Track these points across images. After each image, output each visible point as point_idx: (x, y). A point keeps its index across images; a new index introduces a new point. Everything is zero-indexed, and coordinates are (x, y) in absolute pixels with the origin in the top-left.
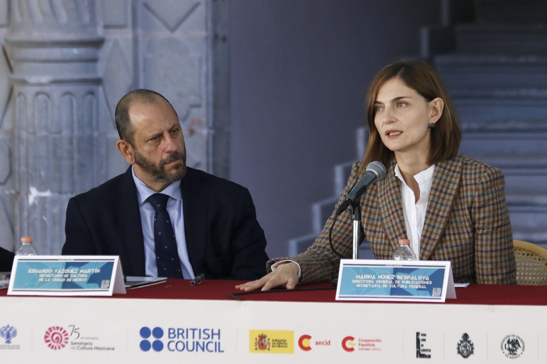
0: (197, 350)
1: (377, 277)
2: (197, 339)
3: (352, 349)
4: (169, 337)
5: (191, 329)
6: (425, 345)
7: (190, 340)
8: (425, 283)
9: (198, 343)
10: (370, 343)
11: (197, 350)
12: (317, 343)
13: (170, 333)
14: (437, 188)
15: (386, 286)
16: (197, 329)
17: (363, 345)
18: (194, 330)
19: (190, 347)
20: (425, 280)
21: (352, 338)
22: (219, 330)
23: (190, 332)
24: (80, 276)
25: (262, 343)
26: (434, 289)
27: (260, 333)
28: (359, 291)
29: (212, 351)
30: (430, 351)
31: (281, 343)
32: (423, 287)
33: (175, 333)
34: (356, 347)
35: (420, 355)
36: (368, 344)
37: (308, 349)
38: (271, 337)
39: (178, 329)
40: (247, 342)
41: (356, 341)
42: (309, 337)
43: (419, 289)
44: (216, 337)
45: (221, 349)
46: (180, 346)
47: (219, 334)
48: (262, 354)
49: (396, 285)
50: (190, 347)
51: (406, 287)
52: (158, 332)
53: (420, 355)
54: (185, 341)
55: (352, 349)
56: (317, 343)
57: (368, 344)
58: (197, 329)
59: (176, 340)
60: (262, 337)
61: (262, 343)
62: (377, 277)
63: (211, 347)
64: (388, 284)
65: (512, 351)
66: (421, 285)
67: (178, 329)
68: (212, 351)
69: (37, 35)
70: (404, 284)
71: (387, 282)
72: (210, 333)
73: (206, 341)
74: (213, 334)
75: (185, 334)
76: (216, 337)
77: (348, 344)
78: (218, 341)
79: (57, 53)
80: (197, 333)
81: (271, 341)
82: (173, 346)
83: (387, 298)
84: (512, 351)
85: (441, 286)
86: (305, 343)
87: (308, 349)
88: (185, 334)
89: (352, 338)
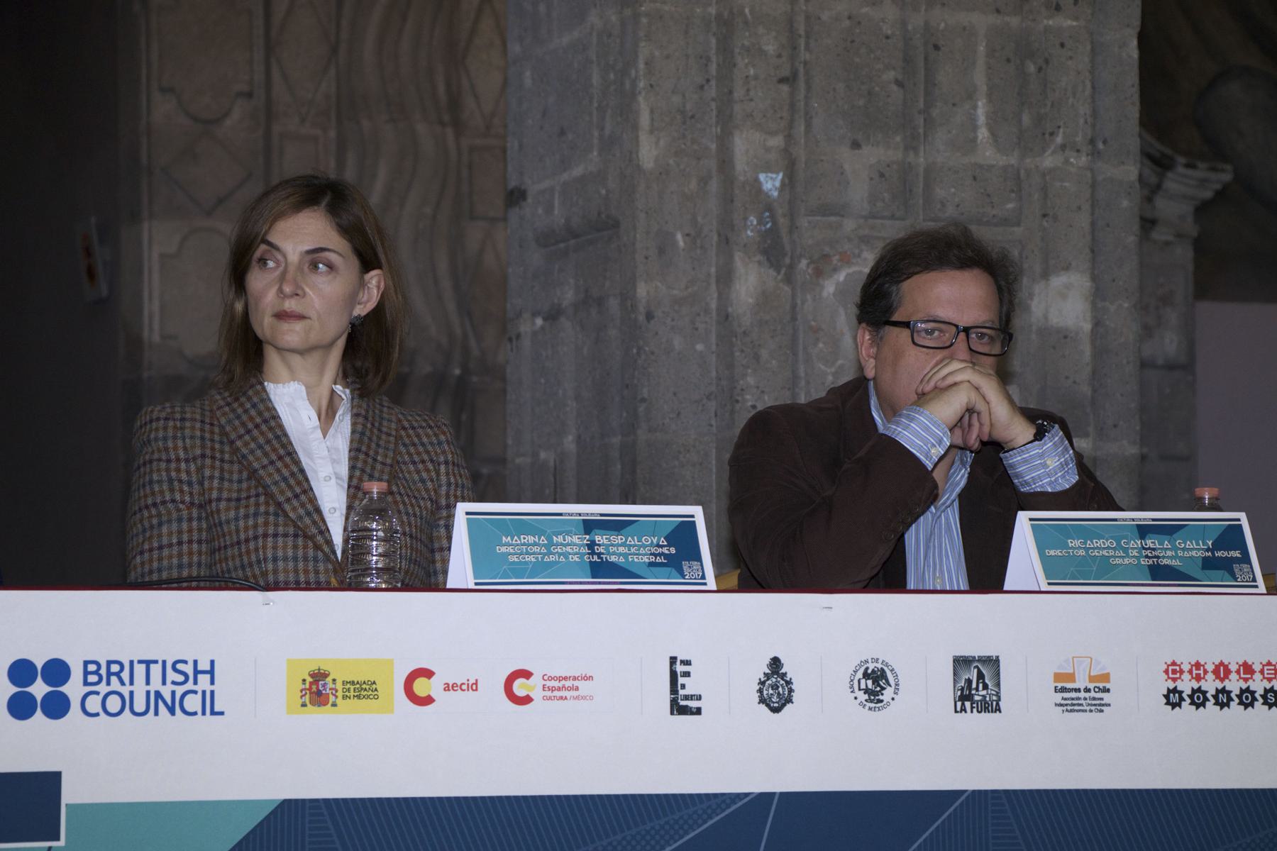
0: (156, 713)
1: (549, 539)
2: (156, 683)
3: (526, 700)
4: (86, 683)
5: (140, 662)
6: (690, 686)
7: (140, 689)
8: (660, 550)
9: (158, 694)
10: (568, 684)
11: (156, 713)
12: (447, 688)
13: (86, 673)
15: (576, 558)
16: (156, 662)
17: (552, 689)
18: (148, 663)
19: (140, 705)
20: (658, 546)
21: (526, 674)
22: (212, 662)
23: (140, 670)
25: (317, 689)
26: (685, 565)
27: (314, 667)
29: (195, 714)
30: (699, 698)
31: (363, 690)
32: (659, 560)
34: (537, 694)
35: (678, 709)
37: (428, 700)
38: (339, 675)
39: (109, 663)
41: (536, 681)
42: (428, 674)
43: (651, 564)
44: (204, 680)
45: (216, 709)
46: (114, 704)
47: (211, 672)
48: (318, 717)
49: (599, 555)
50: (140, 705)
51: (622, 560)
52: (57, 671)
53: (678, 709)
54: (125, 691)
55: (526, 700)
56: (447, 688)
57: (561, 687)
58: (156, 662)
59: (103, 688)
60: (319, 676)
61: (317, 689)
62: (549, 539)
63: (193, 703)
64: (582, 555)
66: (655, 555)
67: (109, 663)
68: (195, 714)
70: (614, 553)
71: (576, 550)
72: (189, 669)
73: (179, 690)
74: (196, 672)
75: (125, 675)
76: (204, 680)
77: (520, 688)
78: (208, 688)
80: (156, 670)
81: (339, 686)
82: (94, 704)
83: (581, 583)
85: (698, 558)
86: (421, 687)
87: (428, 700)
88: (125, 675)
89: (526, 674)
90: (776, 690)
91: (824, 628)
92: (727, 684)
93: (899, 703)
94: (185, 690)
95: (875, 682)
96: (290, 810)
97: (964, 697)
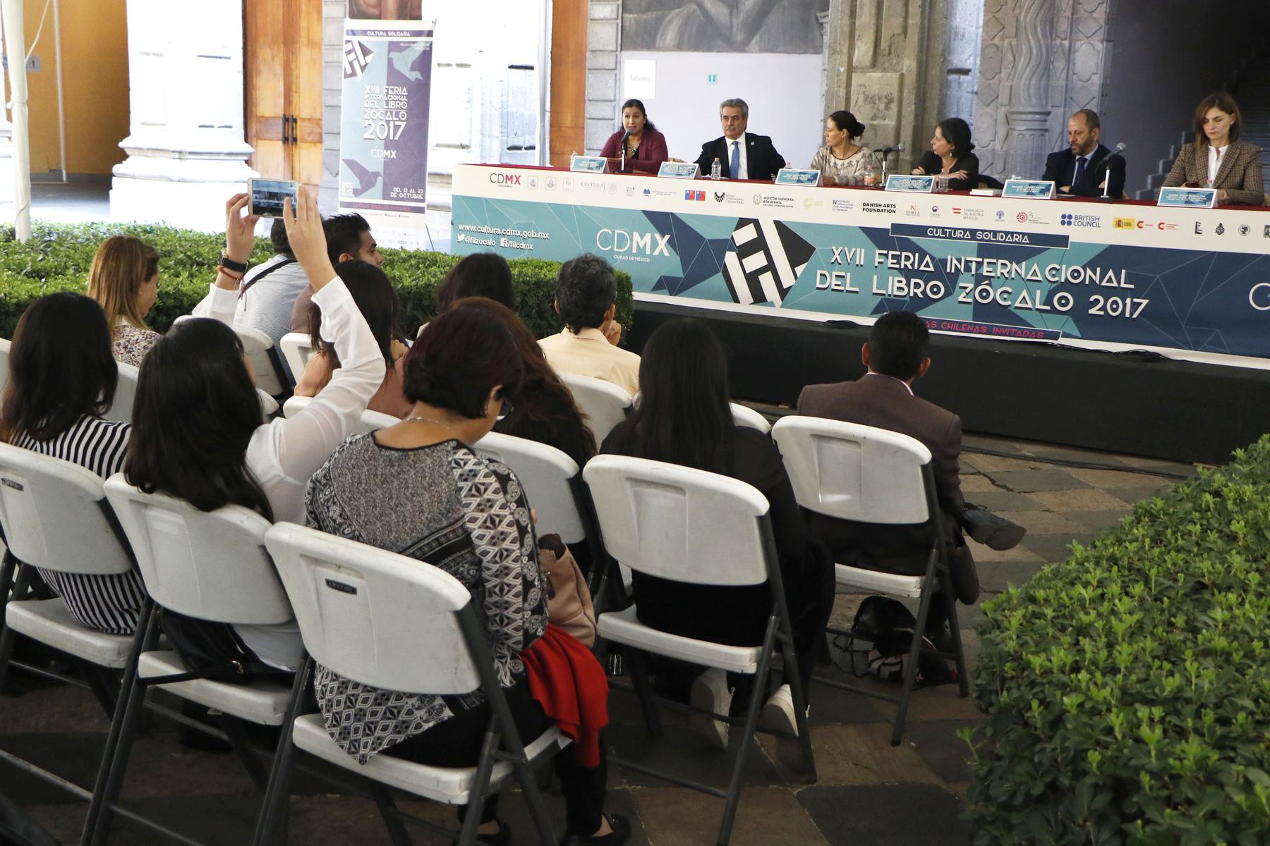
14: (1228, 155)
24: (1035, 190)
31: (1129, 224)
36: (1171, 226)
40: (1112, 223)
52: (1070, 217)
57: (1171, 226)
61: (1119, 224)
90: (1220, 230)
92: (1209, 228)
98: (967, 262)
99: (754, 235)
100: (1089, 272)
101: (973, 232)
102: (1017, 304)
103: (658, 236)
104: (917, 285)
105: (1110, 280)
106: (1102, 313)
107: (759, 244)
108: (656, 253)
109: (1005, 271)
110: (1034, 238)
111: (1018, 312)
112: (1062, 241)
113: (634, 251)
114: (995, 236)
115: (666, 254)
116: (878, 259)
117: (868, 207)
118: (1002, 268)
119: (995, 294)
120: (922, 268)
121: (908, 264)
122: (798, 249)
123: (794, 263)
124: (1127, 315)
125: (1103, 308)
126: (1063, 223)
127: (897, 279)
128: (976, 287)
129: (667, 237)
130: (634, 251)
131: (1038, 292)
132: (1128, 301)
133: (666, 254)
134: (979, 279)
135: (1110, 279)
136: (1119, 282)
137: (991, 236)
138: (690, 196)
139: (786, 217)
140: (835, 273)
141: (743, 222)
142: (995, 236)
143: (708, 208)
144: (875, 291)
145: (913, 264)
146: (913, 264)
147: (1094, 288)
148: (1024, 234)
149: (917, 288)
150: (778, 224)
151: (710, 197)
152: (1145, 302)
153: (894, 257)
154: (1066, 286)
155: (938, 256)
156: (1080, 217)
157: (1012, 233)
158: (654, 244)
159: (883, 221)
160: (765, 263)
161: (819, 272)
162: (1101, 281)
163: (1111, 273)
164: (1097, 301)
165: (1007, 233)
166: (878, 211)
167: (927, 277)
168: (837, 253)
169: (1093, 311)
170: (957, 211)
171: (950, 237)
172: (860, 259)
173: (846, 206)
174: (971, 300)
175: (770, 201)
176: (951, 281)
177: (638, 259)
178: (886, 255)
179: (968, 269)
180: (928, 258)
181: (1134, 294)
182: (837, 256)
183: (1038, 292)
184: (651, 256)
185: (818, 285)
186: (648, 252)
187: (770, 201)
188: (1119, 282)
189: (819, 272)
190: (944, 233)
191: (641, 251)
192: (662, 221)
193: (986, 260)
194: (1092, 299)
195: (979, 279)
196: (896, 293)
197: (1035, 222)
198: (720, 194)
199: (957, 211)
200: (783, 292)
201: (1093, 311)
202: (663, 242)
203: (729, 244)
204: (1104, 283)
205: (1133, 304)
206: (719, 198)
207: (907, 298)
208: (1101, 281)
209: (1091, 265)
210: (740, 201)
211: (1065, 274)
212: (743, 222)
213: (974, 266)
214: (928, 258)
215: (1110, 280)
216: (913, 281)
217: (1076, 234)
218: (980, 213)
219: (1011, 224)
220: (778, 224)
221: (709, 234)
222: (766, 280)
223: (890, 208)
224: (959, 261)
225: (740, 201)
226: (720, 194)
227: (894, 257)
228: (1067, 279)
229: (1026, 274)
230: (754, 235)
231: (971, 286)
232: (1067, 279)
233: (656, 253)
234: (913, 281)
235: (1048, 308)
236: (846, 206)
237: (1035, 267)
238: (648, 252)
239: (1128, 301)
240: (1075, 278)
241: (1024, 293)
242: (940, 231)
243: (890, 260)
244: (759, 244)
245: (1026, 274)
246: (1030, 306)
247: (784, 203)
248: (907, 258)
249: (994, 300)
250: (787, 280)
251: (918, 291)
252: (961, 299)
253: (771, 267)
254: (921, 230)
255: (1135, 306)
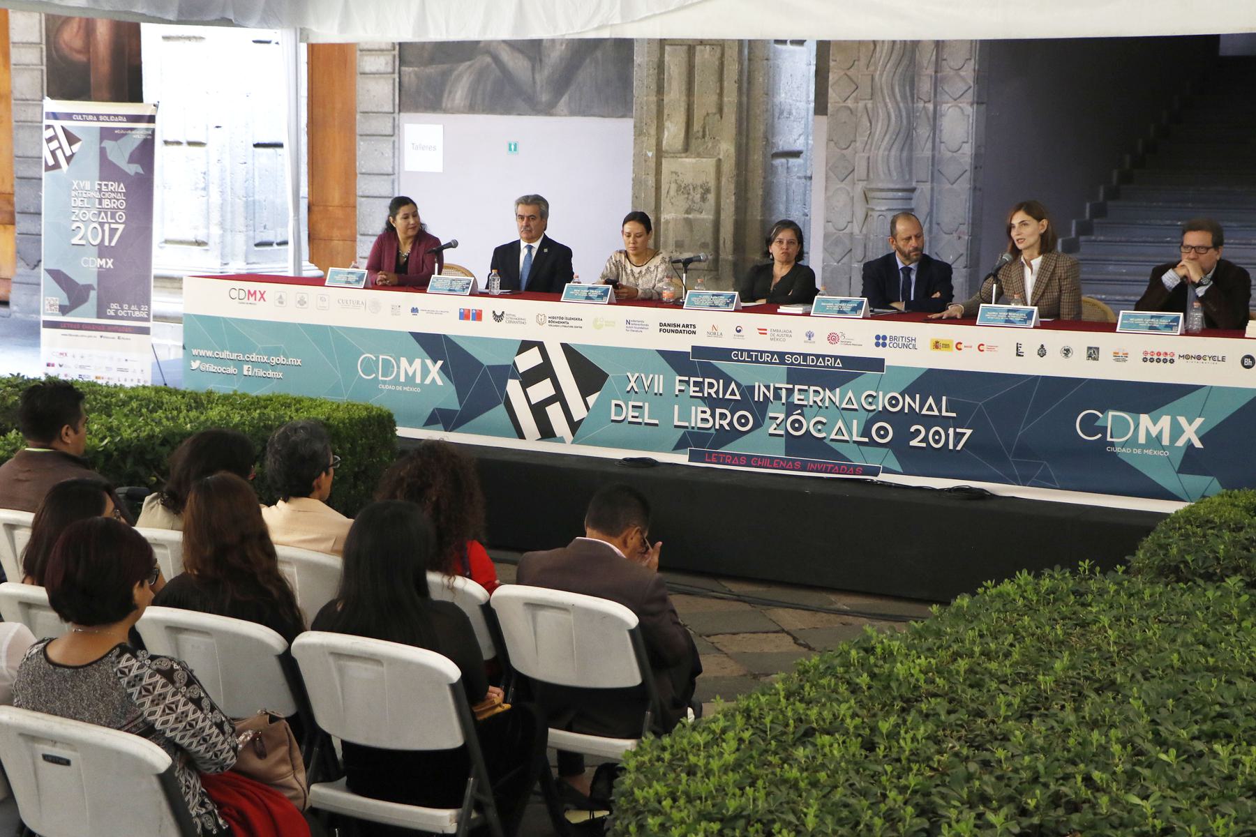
14: (1043, 267)
24: (847, 307)
25: (937, 345)
28: (989, 320)
31: (947, 346)
33: (893, 338)
36: (991, 348)
40: (929, 344)
48: (936, 351)
52: (884, 338)
57: (991, 348)
61: (937, 345)
65: (1066, 355)
69: (880, 185)
79: (891, 195)
84: (1066, 355)
90: (1042, 352)
91: (1057, 339)
92: (1030, 350)
93: (1073, 357)
94: (909, 343)
95: (1067, 352)
96: (930, 371)
97: (1090, 356)
98: (776, 389)
99: (539, 360)
100: (908, 399)
101: (781, 355)
102: (833, 436)
103: (429, 362)
104: (723, 416)
105: (930, 408)
106: (924, 445)
107: (544, 371)
108: (428, 381)
109: (818, 400)
110: (848, 361)
111: (833, 445)
112: (877, 364)
113: (402, 379)
114: (805, 360)
115: (440, 382)
116: (678, 387)
117: (665, 328)
118: (813, 395)
119: (809, 425)
120: (727, 396)
121: (712, 391)
122: (589, 375)
123: (585, 393)
124: (951, 447)
125: (925, 440)
126: (877, 345)
127: (700, 409)
128: (787, 417)
129: (440, 363)
130: (402, 379)
131: (855, 422)
132: (951, 431)
133: (440, 382)
134: (791, 408)
135: (930, 407)
136: (940, 411)
137: (801, 360)
138: (464, 315)
139: (576, 339)
140: (631, 404)
141: (525, 346)
142: (805, 360)
143: (486, 329)
144: (677, 423)
145: (717, 392)
146: (717, 392)
147: (914, 417)
148: (836, 357)
149: (724, 420)
150: (566, 348)
151: (487, 316)
152: (969, 432)
153: (696, 384)
154: (883, 415)
155: (744, 383)
156: (895, 338)
157: (824, 357)
158: (425, 372)
159: (682, 344)
160: (553, 392)
161: (614, 402)
162: (921, 408)
163: (931, 400)
164: (918, 431)
165: (818, 356)
166: (677, 332)
167: (734, 406)
168: (633, 380)
169: (914, 443)
170: (763, 331)
171: (757, 361)
172: (659, 387)
173: (641, 326)
174: (782, 432)
175: (554, 321)
176: (760, 410)
177: (407, 389)
178: (688, 382)
179: (777, 397)
180: (733, 385)
181: (957, 423)
182: (632, 383)
183: (855, 422)
184: (422, 385)
185: (613, 418)
186: (418, 381)
187: (554, 321)
188: (940, 411)
189: (614, 402)
190: (750, 356)
191: (410, 380)
192: (434, 345)
193: (797, 387)
194: (912, 429)
195: (791, 408)
196: (700, 425)
197: (847, 343)
198: (499, 313)
199: (763, 331)
200: (574, 426)
201: (914, 443)
202: (435, 369)
203: (510, 371)
204: (924, 412)
205: (956, 434)
206: (498, 318)
207: (713, 431)
208: (921, 408)
209: (910, 391)
210: (522, 321)
211: (882, 402)
212: (525, 346)
213: (784, 393)
214: (733, 385)
215: (930, 408)
216: (718, 411)
217: (893, 357)
218: (788, 333)
219: (821, 346)
220: (566, 348)
221: (488, 359)
222: (554, 412)
223: (689, 329)
224: (768, 387)
225: (522, 321)
226: (499, 313)
227: (696, 384)
228: (884, 407)
229: (841, 402)
230: (539, 360)
231: (782, 416)
232: (884, 407)
233: (428, 381)
234: (718, 411)
235: (866, 440)
236: (641, 326)
237: (850, 394)
238: (418, 381)
239: (951, 431)
240: (894, 406)
241: (840, 424)
242: (745, 354)
243: (692, 388)
244: (544, 371)
245: (841, 402)
246: (846, 438)
247: (572, 323)
248: (711, 385)
249: (808, 431)
250: (579, 412)
251: (725, 423)
252: (771, 431)
253: (559, 397)
254: (725, 354)
255: (958, 436)
